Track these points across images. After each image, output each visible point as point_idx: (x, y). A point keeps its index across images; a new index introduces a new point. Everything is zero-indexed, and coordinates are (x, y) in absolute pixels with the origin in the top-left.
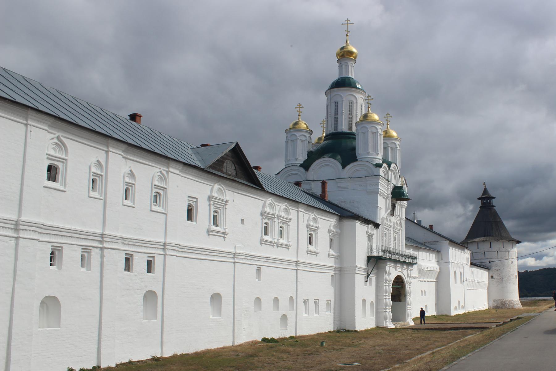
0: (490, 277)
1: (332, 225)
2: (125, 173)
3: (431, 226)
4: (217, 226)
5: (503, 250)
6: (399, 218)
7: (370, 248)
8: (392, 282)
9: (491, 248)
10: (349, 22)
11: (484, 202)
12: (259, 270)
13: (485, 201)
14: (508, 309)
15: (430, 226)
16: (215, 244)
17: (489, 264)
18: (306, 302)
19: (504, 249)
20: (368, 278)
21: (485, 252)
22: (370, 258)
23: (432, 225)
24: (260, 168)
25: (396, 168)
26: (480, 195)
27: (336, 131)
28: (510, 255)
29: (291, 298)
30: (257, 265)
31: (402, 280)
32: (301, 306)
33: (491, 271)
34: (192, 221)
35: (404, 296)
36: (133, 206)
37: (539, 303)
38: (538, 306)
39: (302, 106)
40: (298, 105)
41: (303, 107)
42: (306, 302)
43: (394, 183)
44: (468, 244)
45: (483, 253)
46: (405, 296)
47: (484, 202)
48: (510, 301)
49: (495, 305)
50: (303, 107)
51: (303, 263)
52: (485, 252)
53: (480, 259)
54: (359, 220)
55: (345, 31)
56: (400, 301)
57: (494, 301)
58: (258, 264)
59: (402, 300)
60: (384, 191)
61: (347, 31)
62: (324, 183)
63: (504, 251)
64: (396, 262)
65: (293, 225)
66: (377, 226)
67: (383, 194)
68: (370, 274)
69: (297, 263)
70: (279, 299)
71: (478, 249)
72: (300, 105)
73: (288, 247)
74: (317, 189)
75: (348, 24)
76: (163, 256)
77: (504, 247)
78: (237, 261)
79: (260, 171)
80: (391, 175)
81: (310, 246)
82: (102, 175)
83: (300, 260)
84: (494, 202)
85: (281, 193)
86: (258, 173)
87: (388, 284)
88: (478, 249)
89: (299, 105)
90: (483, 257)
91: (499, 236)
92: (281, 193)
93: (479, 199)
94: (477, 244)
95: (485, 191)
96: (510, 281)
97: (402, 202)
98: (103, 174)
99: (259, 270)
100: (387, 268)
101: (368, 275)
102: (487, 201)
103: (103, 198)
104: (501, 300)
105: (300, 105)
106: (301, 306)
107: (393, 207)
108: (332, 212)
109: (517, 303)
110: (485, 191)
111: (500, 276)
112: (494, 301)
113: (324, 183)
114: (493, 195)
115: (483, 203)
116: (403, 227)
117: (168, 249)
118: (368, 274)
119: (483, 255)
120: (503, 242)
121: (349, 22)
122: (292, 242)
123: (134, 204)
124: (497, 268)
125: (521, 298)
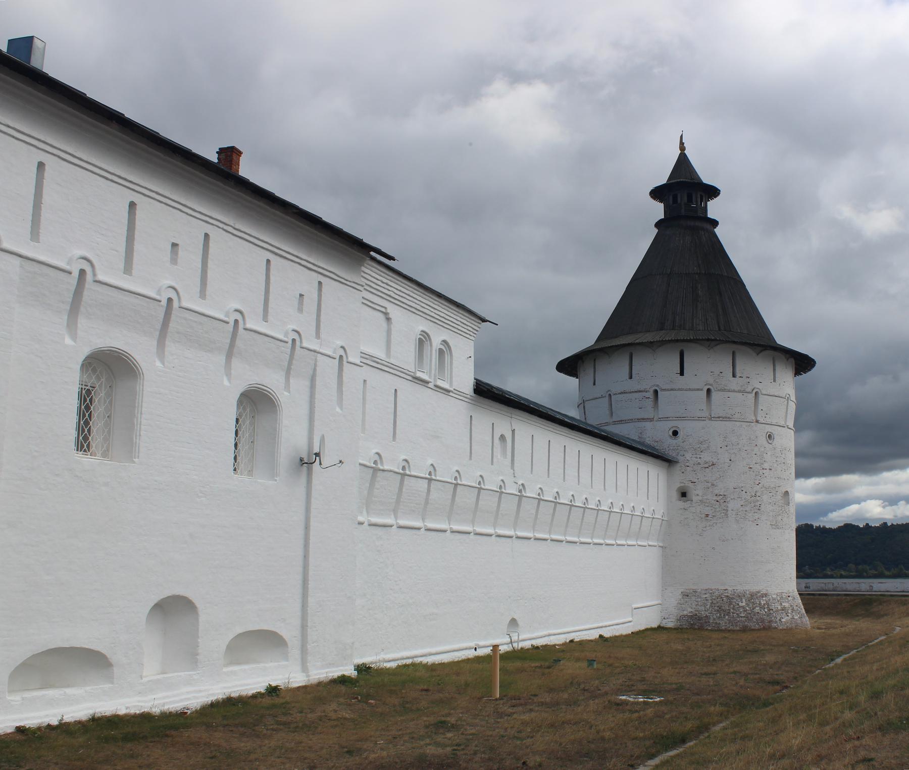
0: (675, 495)
3: (230, 154)
5: (735, 383)
9: (682, 373)
14: (745, 630)
15: (222, 151)
17: (673, 442)
19: (737, 379)
21: (656, 392)
28: (760, 407)
33: (677, 469)
37: (880, 604)
38: (879, 616)
44: (595, 360)
45: (650, 394)
48: (753, 596)
49: (688, 611)
52: (656, 392)
53: (639, 420)
57: (685, 595)
63: (739, 391)
71: (631, 377)
77: (738, 375)
88: (631, 377)
90: (649, 412)
91: (720, 329)
94: (628, 357)
95: (683, 163)
96: (757, 516)
104: (717, 593)
109: (786, 605)
110: (683, 163)
111: (717, 492)
112: (685, 595)
119: (650, 403)
120: (734, 353)
124: (706, 457)
125: (816, 584)
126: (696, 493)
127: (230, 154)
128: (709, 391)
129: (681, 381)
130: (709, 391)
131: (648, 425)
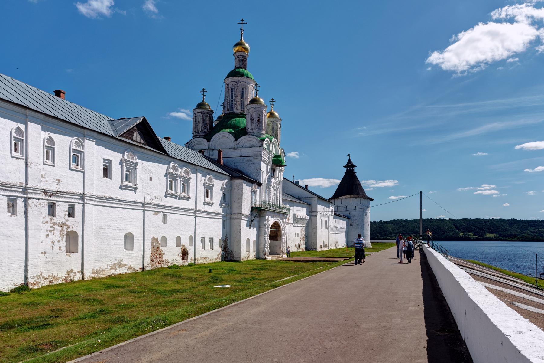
0: (350, 225)
1: (225, 183)
2: (45, 138)
3: (306, 186)
4: (130, 182)
6: (278, 179)
7: (254, 200)
8: (270, 227)
10: (243, 22)
11: (348, 169)
12: (164, 215)
13: (349, 169)
15: (306, 186)
16: (128, 195)
18: (203, 240)
20: (251, 223)
21: (346, 207)
22: (253, 209)
23: (307, 185)
24: (170, 139)
25: (277, 142)
26: (345, 164)
27: (232, 112)
29: (191, 237)
30: (163, 212)
31: (279, 225)
32: (199, 244)
33: (350, 220)
34: (107, 178)
35: (280, 236)
36: (54, 165)
39: (205, 91)
40: (202, 90)
41: (206, 92)
42: (203, 240)
43: (274, 153)
45: (345, 207)
46: (281, 236)
47: (348, 169)
50: (206, 92)
51: (201, 211)
52: (346, 207)
54: (245, 180)
55: (241, 29)
56: (277, 240)
58: (164, 211)
59: (279, 239)
60: (266, 159)
61: (242, 30)
62: (220, 152)
64: (274, 212)
65: (192, 183)
66: (260, 185)
67: (265, 161)
68: (253, 220)
69: (195, 211)
70: (181, 237)
71: (342, 203)
72: (204, 89)
73: (188, 199)
74: (215, 155)
75: (242, 23)
76: (82, 204)
78: (146, 209)
79: (170, 141)
80: (272, 147)
81: (206, 199)
82: (23, 140)
83: (198, 208)
84: (356, 170)
85: (181, 157)
86: (168, 142)
87: (267, 228)
88: (342, 203)
89: (204, 90)
92: (181, 157)
93: (344, 167)
95: (350, 162)
97: (281, 167)
98: (24, 138)
99: (164, 215)
100: (267, 217)
101: (252, 221)
102: (350, 169)
103: (24, 158)
105: (204, 89)
106: (199, 244)
107: (274, 171)
108: (224, 173)
110: (350, 162)
113: (220, 152)
114: (355, 164)
115: (347, 170)
116: (281, 186)
117: (86, 199)
118: (251, 220)
121: (243, 22)
122: (192, 195)
123: (54, 163)
124: (355, 218)
126: (353, 224)
127: (306, 186)
128: (356, 206)
129: (351, 205)
130: (356, 206)
131: (345, 212)
